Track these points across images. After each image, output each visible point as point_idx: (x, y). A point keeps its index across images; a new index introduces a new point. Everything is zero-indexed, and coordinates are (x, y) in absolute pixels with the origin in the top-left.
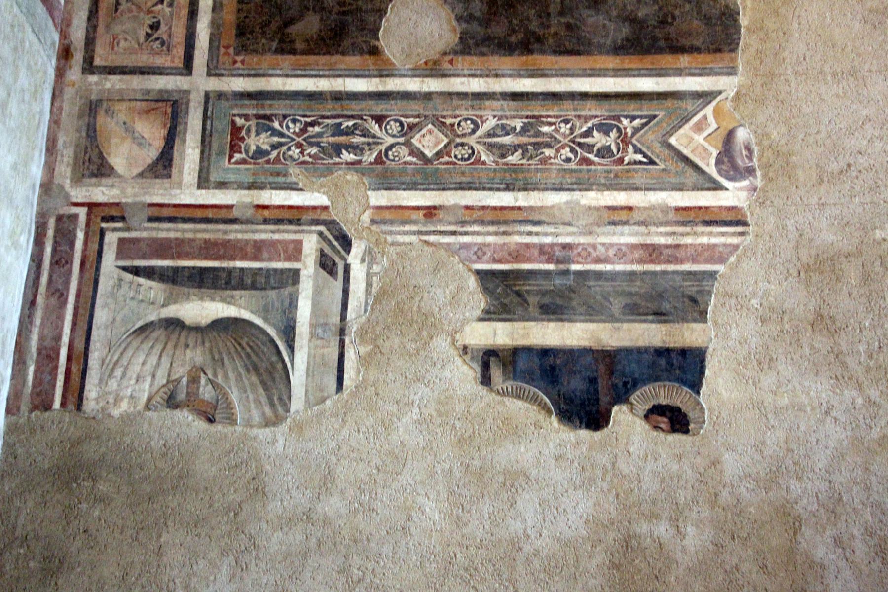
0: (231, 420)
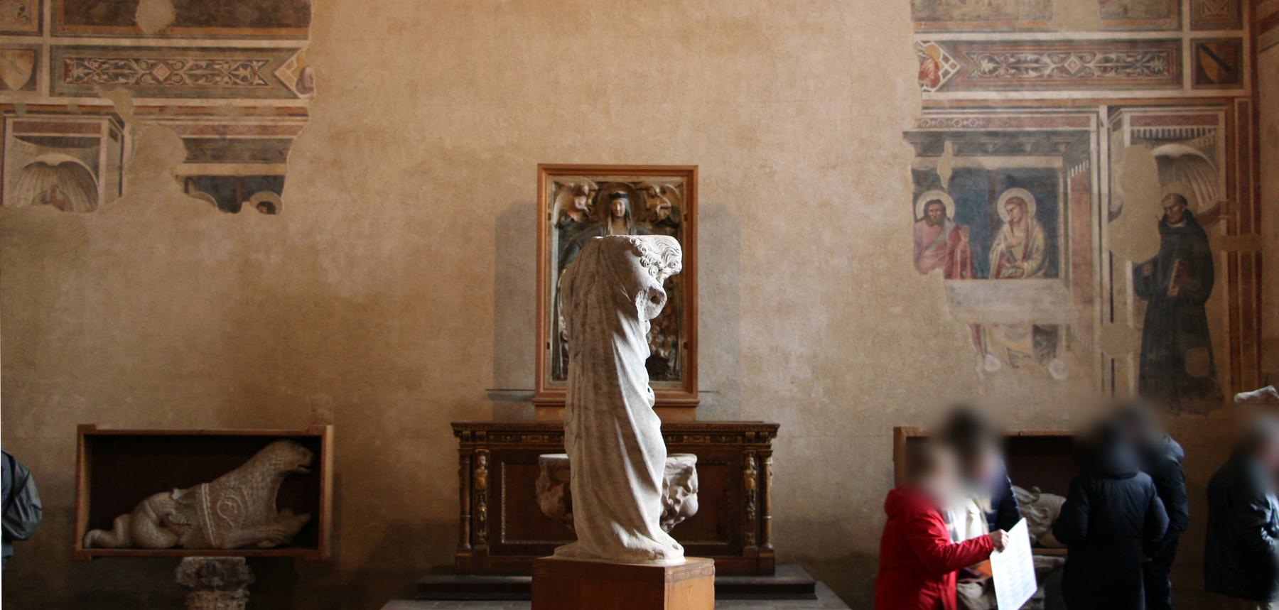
0: (71, 209)
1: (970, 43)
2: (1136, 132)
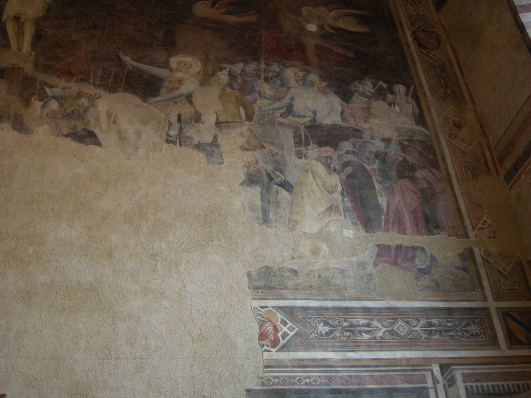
1: (305, 309)
2: (469, 387)
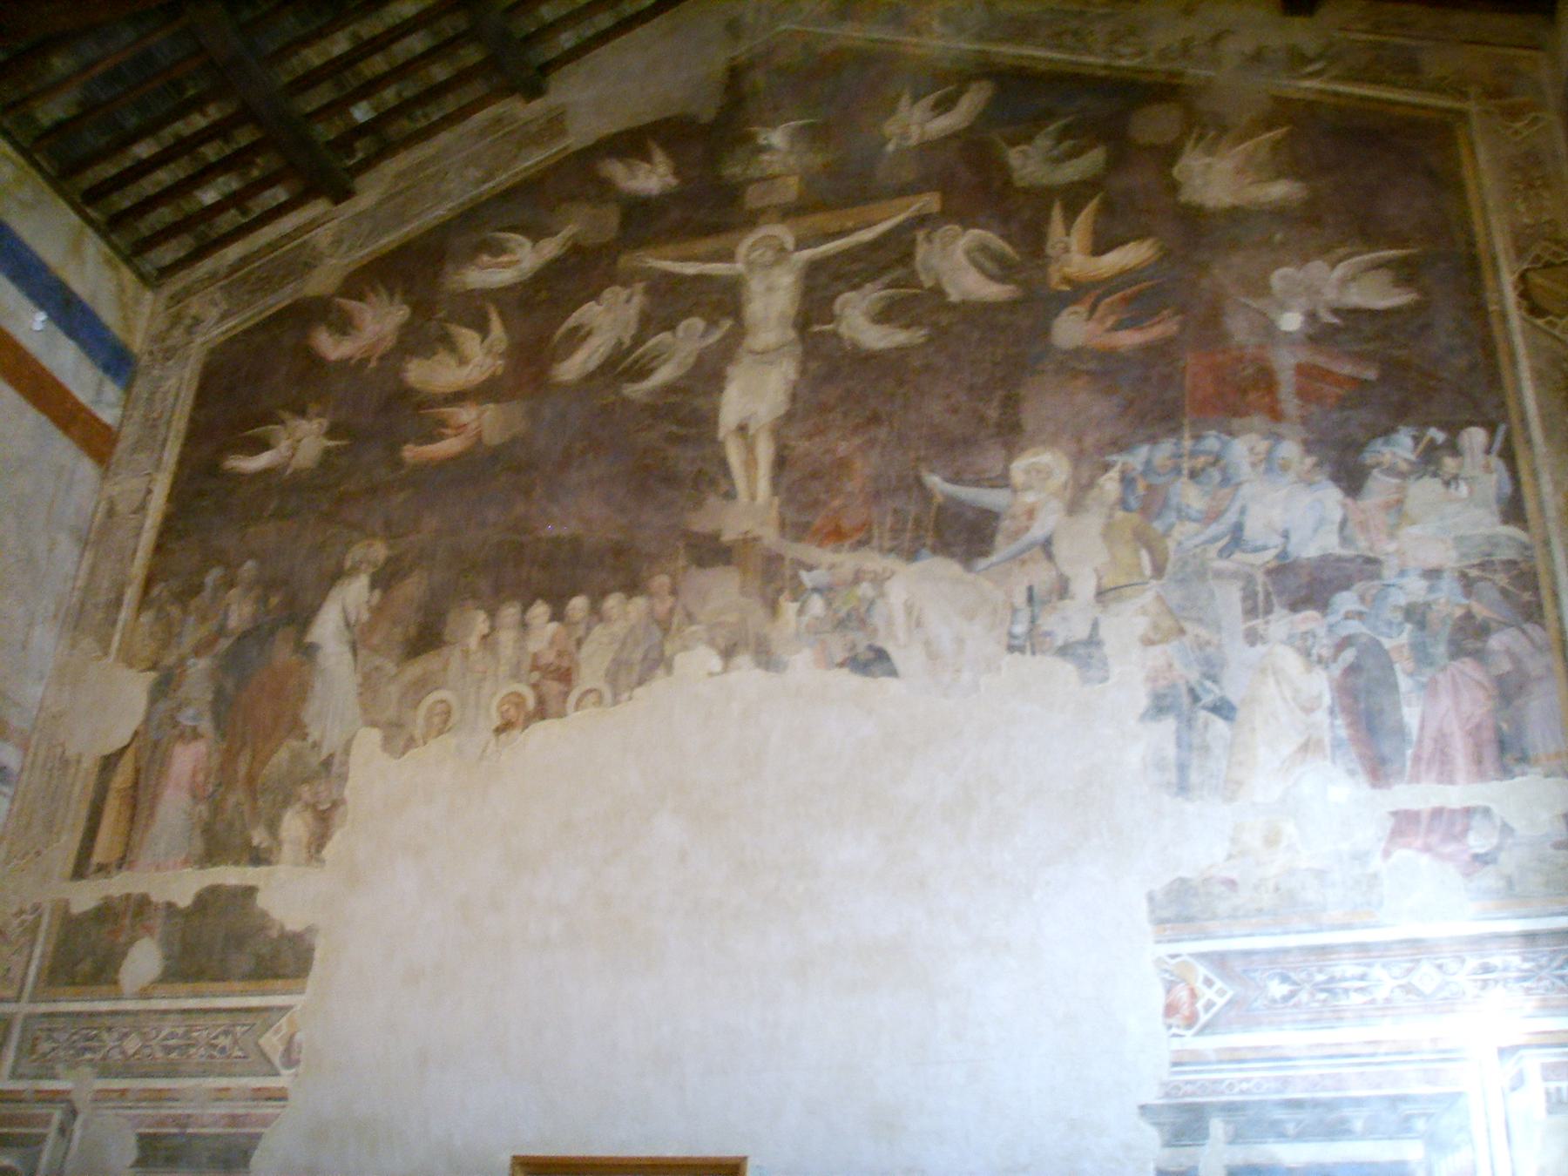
1: (1247, 954)
